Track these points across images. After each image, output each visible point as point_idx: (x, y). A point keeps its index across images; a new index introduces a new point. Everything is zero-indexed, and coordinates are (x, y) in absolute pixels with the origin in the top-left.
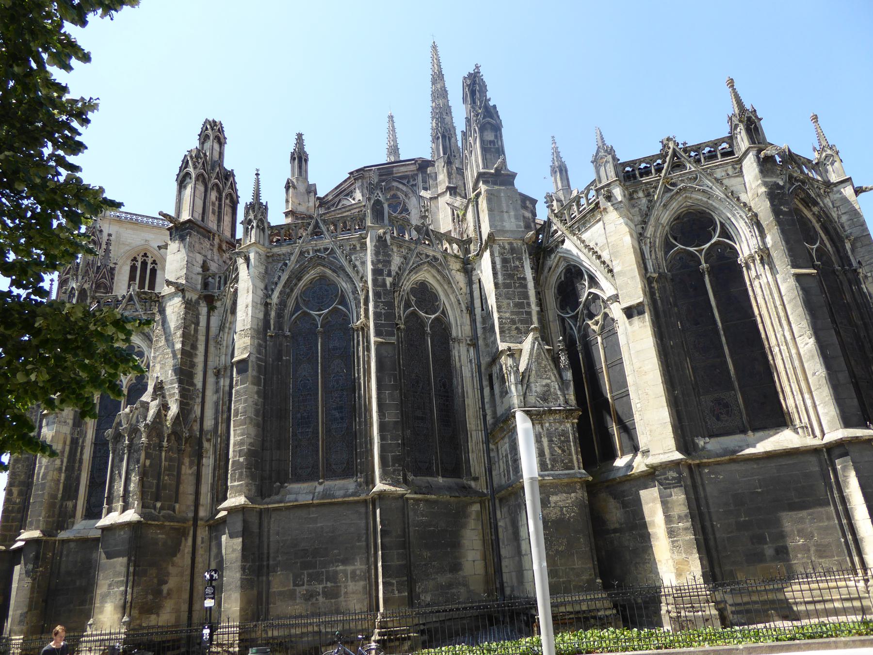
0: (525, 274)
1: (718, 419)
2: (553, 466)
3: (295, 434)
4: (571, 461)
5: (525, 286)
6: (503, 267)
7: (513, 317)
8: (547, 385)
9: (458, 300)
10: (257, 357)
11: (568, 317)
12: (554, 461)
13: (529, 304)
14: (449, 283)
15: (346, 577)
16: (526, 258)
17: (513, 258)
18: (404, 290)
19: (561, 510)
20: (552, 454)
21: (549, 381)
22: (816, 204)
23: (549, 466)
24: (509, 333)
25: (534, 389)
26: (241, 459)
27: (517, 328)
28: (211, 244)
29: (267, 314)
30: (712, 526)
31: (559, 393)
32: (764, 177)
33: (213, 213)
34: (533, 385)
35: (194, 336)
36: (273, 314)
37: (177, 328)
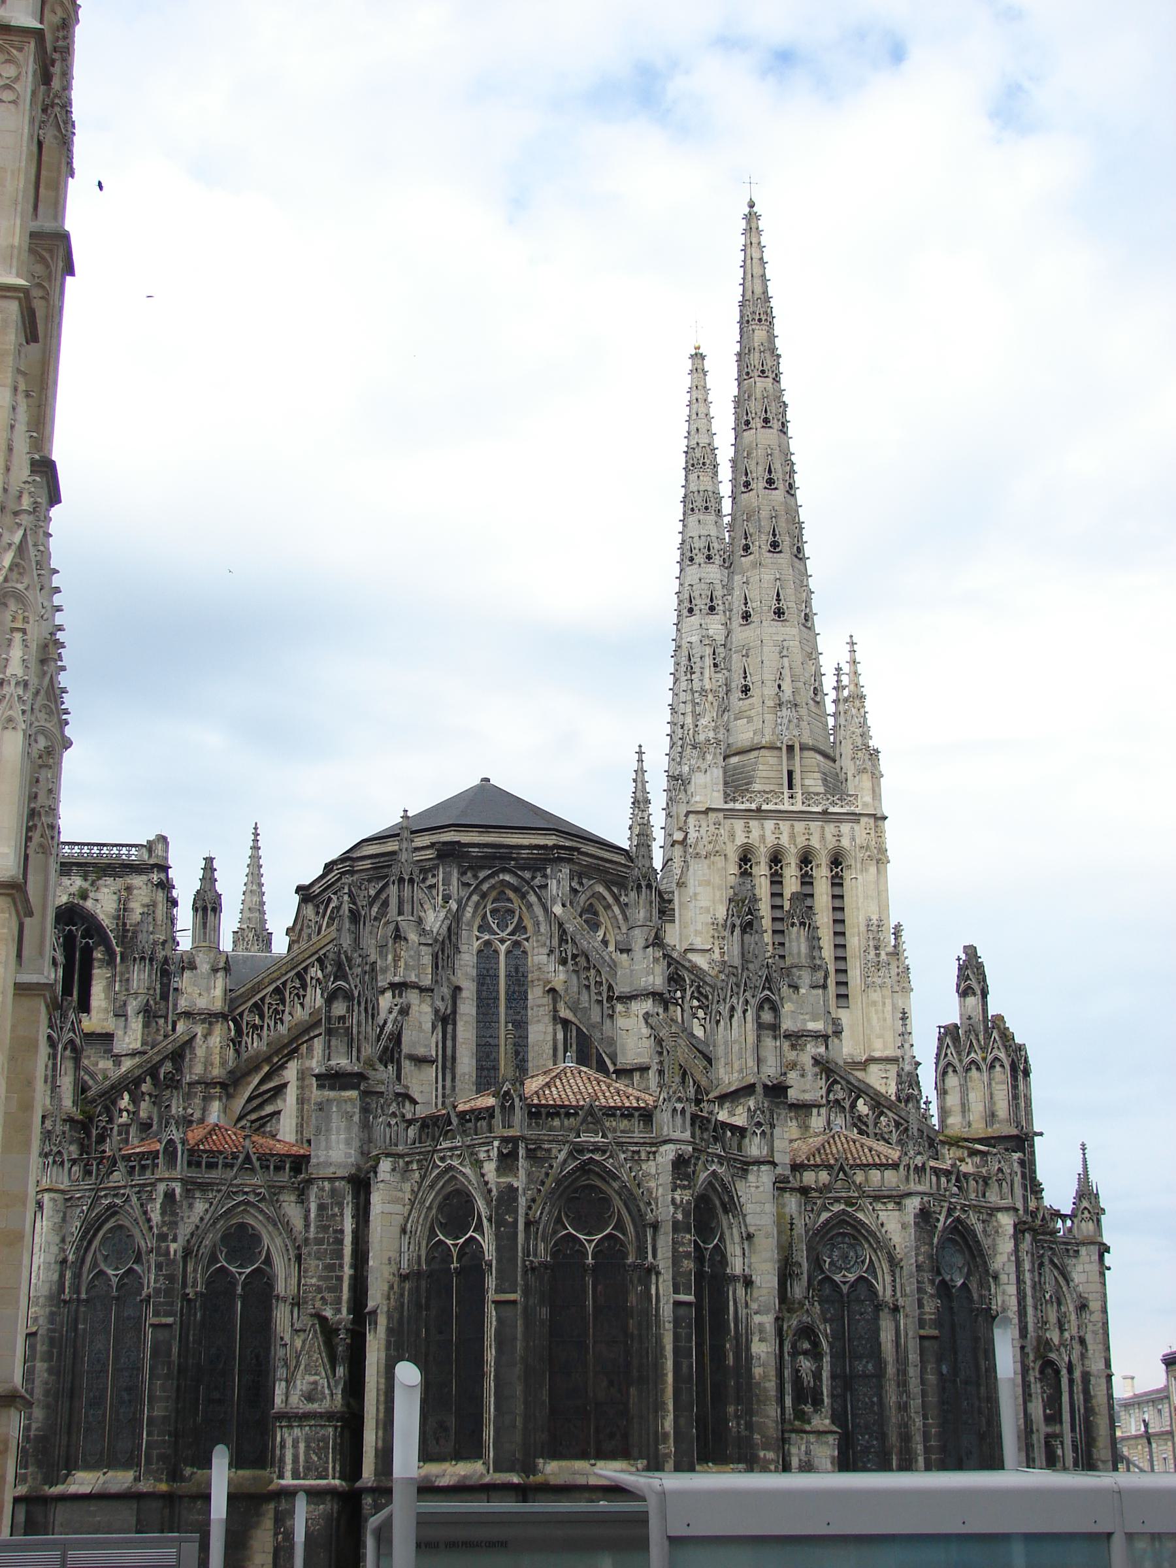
4: (326, 1469)
5: (340, 1242)
6: (319, 1216)
7: (320, 1283)
8: (315, 1383)
12: (308, 1469)
13: (341, 1266)
16: (348, 1204)
17: (332, 1203)
20: (306, 1461)
21: (318, 1378)
27: (322, 1298)
29: (62, 1276)
31: (327, 1391)
32: (498, 1177)
36: (68, 1274)
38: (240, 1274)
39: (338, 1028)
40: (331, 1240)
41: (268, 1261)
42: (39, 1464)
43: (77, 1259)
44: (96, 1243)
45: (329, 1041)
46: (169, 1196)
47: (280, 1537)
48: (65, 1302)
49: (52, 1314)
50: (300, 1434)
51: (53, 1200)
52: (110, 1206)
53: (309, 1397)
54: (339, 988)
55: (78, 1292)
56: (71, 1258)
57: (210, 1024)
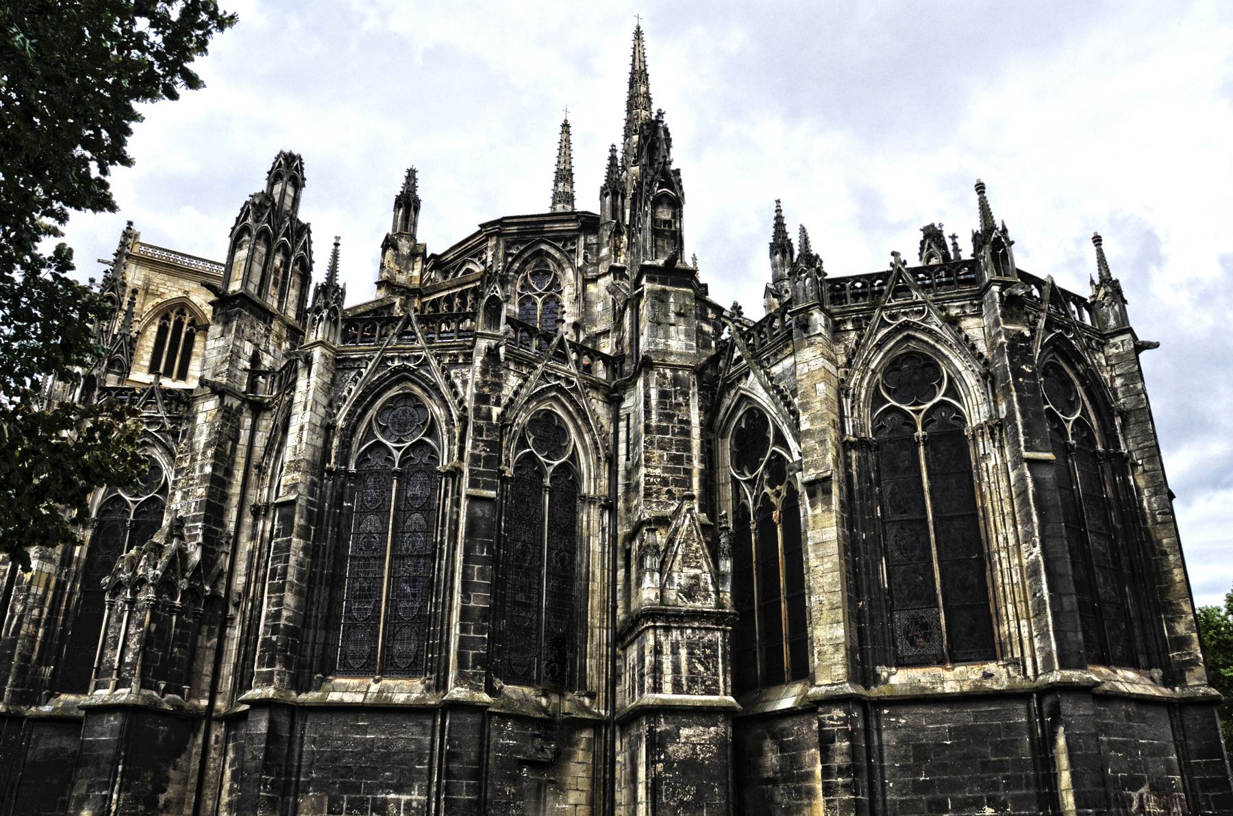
0: (689, 416)
1: (912, 643)
2: (690, 688)
3: (349, 610)
4: (716, 683)
5: (688, 433)
7: (666, 475)
8: (696, 577)
9: (596, 443)
10: (308, 500)
11: (744, 481)
12: (692, 681)
13: (690, 459)
14: (585, 419)
15: (399, 809)
16: (693, 395)
17: (675, 391)
18: (518, 425)
19: (694, 749)
20: (690, 671)
21: (698, 571)
22: (1082, 360)
23: (685, 688)
24: (657, 498)
25: (676, 581)
26: (274, 638)
27: (669, 492)
28: (266, 329)
29: (327, 442)
30: (884, 785)
31: (711, 588)
33: (275, 284)
34: (675, 575)
35: (230, 456)
36: (336, 442)
37: (208, 445)
38: (548, 465)
39: (665, 231)
40: (676, 430)
41: (574, 457)
42: (287, 663)
43: (347, 428)
44: (372, 413)
45: (656, 241)
46: (492, 353)
47: (660, 766)
48: (330, 471)
49: (313, 483)
50: (680, 638)
51: (323, 355)
52: (396, 371)
53: (690, 592)
54: (665, 195)
55: (345, 462)
56: (341, 423)
57: (408, 298)
